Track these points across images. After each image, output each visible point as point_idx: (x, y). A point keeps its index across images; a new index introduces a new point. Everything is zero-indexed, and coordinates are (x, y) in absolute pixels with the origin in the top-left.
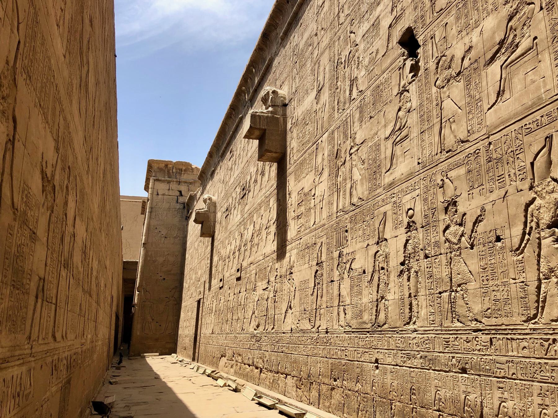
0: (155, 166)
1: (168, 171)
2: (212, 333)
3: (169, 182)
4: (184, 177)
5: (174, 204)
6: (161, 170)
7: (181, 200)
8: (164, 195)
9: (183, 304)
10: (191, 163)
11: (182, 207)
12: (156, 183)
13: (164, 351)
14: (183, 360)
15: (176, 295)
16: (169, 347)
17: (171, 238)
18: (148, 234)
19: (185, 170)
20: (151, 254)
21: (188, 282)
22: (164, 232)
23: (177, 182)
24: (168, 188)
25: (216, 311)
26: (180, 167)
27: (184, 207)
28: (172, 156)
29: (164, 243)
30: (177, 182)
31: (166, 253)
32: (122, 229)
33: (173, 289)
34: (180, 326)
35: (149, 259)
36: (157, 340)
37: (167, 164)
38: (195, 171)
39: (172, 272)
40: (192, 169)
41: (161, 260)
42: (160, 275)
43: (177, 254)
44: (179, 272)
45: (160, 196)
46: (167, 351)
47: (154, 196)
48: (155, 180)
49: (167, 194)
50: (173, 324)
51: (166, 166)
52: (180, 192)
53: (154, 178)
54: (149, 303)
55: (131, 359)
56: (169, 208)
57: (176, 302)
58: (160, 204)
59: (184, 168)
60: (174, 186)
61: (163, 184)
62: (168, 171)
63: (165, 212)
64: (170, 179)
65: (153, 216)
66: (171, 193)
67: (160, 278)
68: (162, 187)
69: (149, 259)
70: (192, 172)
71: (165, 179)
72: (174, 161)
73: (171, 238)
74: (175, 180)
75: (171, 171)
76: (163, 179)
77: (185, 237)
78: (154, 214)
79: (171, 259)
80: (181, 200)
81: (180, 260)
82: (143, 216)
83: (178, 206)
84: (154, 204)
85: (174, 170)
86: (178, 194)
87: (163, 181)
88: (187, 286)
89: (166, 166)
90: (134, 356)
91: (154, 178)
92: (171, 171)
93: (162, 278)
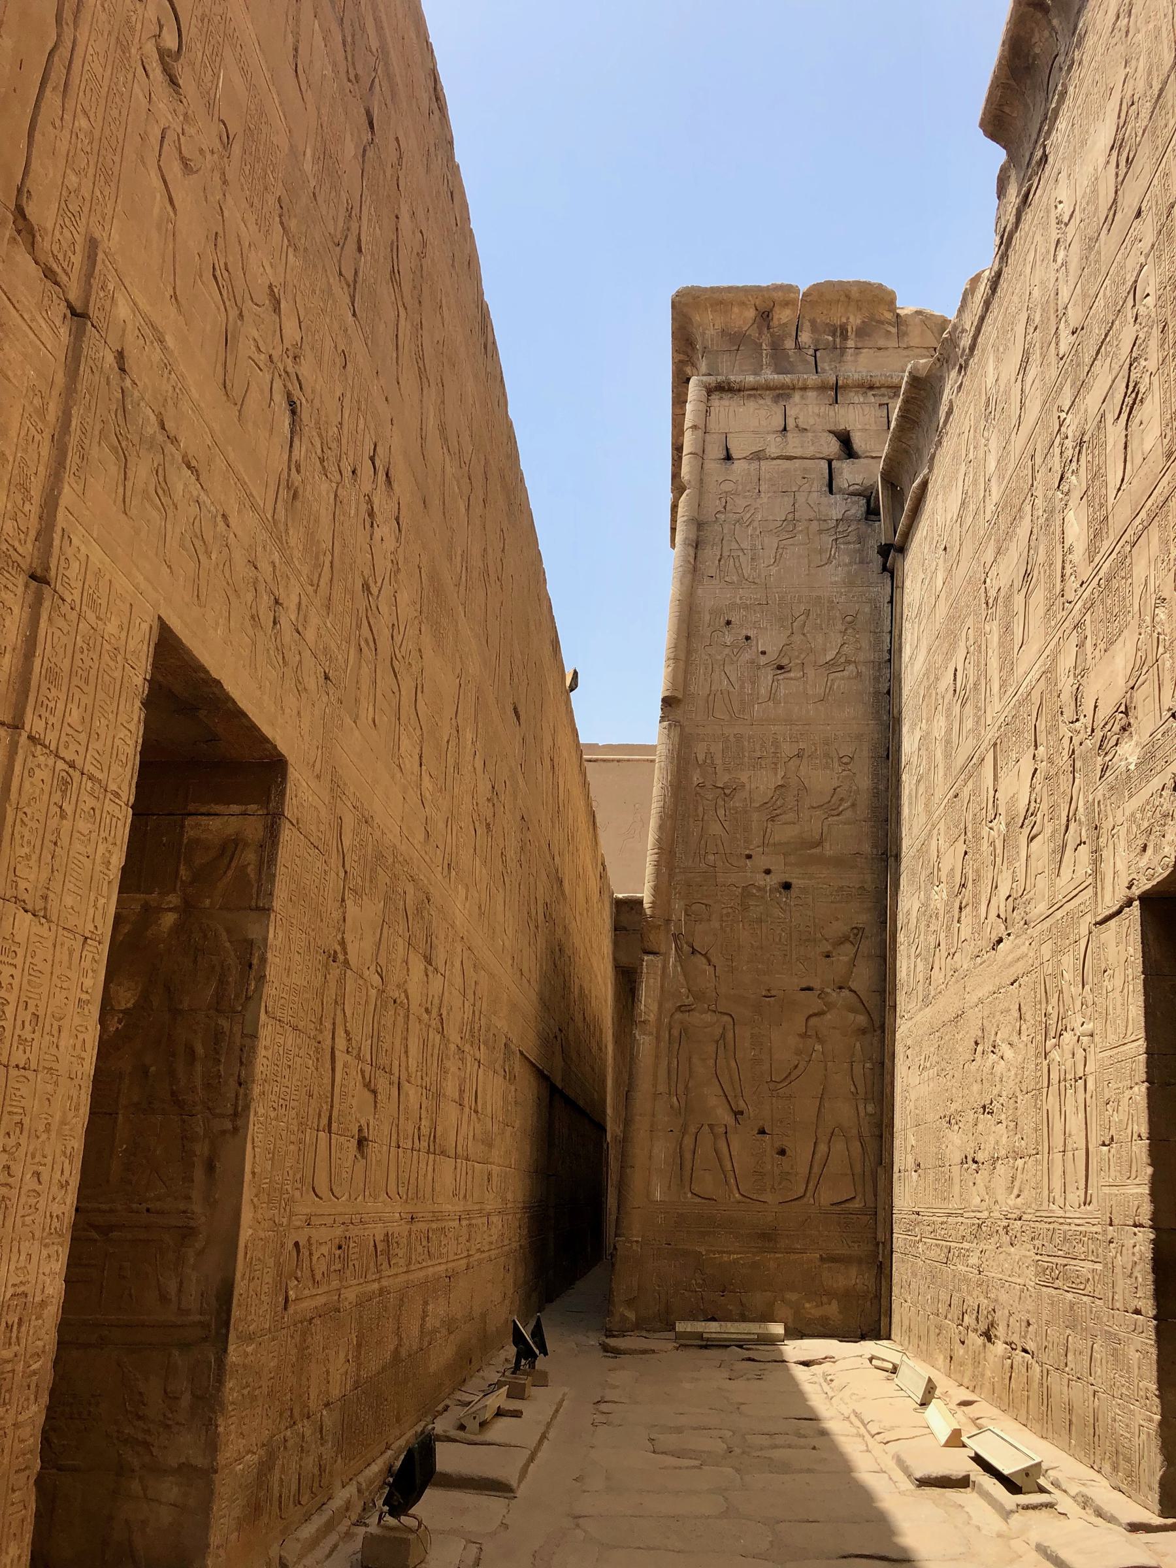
0: (708, 325)
1: (776, 347)
3: (781, 393)
4: (859, 365)
5: (813, 496)
6: (736, 340)
7: (850, 474)
8: (758, 456)
9: (911, 1024)
10: (889, 286)
11: (857, 508)
12: (715, 400)
13: (811, 1309)
14: (1033, 1472)
15: (862, 979)
16: (868, 1320)
17: (811, 672)
18: (689, 652)
19: (861, 333)
20: (708, 753)
21: (951, 860)
22: (770, 641)
23: (822, 388)
24: (778, 422)
26: (837, 316)
27: (872, 512)
28: (793, 260)
29: (772, 696)
30: (822, 388)
31: (788, 749)
32: (573, 686)
33: (844, 940)
34: (902, 1158)
35: (696, 778)
36: (767, 1237)
37: (766, 305)
38: (915, 337)
39: (829, 850)
40: (899, 320)
41: (762, 783)
42: (762, 862)
43: (847, 750)
44: (866, 848)
45: (739, 466)
46: (832, 1309)
47: (712, 466)
48: (710, 391)
49: (773, 451)
50: (856, 1146)
51: (765, 316)
52: (845, 440)
53: (705, 378)
54: (709, 1017)
55: (617, 1352)
56: (791, 522)
57: (862, 1020)
58: (741, 502)
59: (855, 321)
60: (809, 410)
61: (751, 405)
62: (776, 347)
63: (771, 542)
64: (787, 379)
65: (710, 563)
66: (794, 444)
67: (761, 880)
68: (747, 423)
69: (696, 778)
70: (900, 335)
71: (761, 379)
72: (803, 289)
73: (811, 672)
74: (812, 379)
75: (789, 344)
76: (751, 379)
77: (888, 662)
78: (710, 554)
79: (821, 780)
80: (850, 474)
81: (864, 782)
83: (836, 507)
84: (713, 505)
85: (805, 337)
86: (832, 447)
87: (755, 391)
88: (940, 896)
89: (765, 316)
90: (642, 1326)
91: (711, 380)
92: (789, 344)
93: (773, 881)
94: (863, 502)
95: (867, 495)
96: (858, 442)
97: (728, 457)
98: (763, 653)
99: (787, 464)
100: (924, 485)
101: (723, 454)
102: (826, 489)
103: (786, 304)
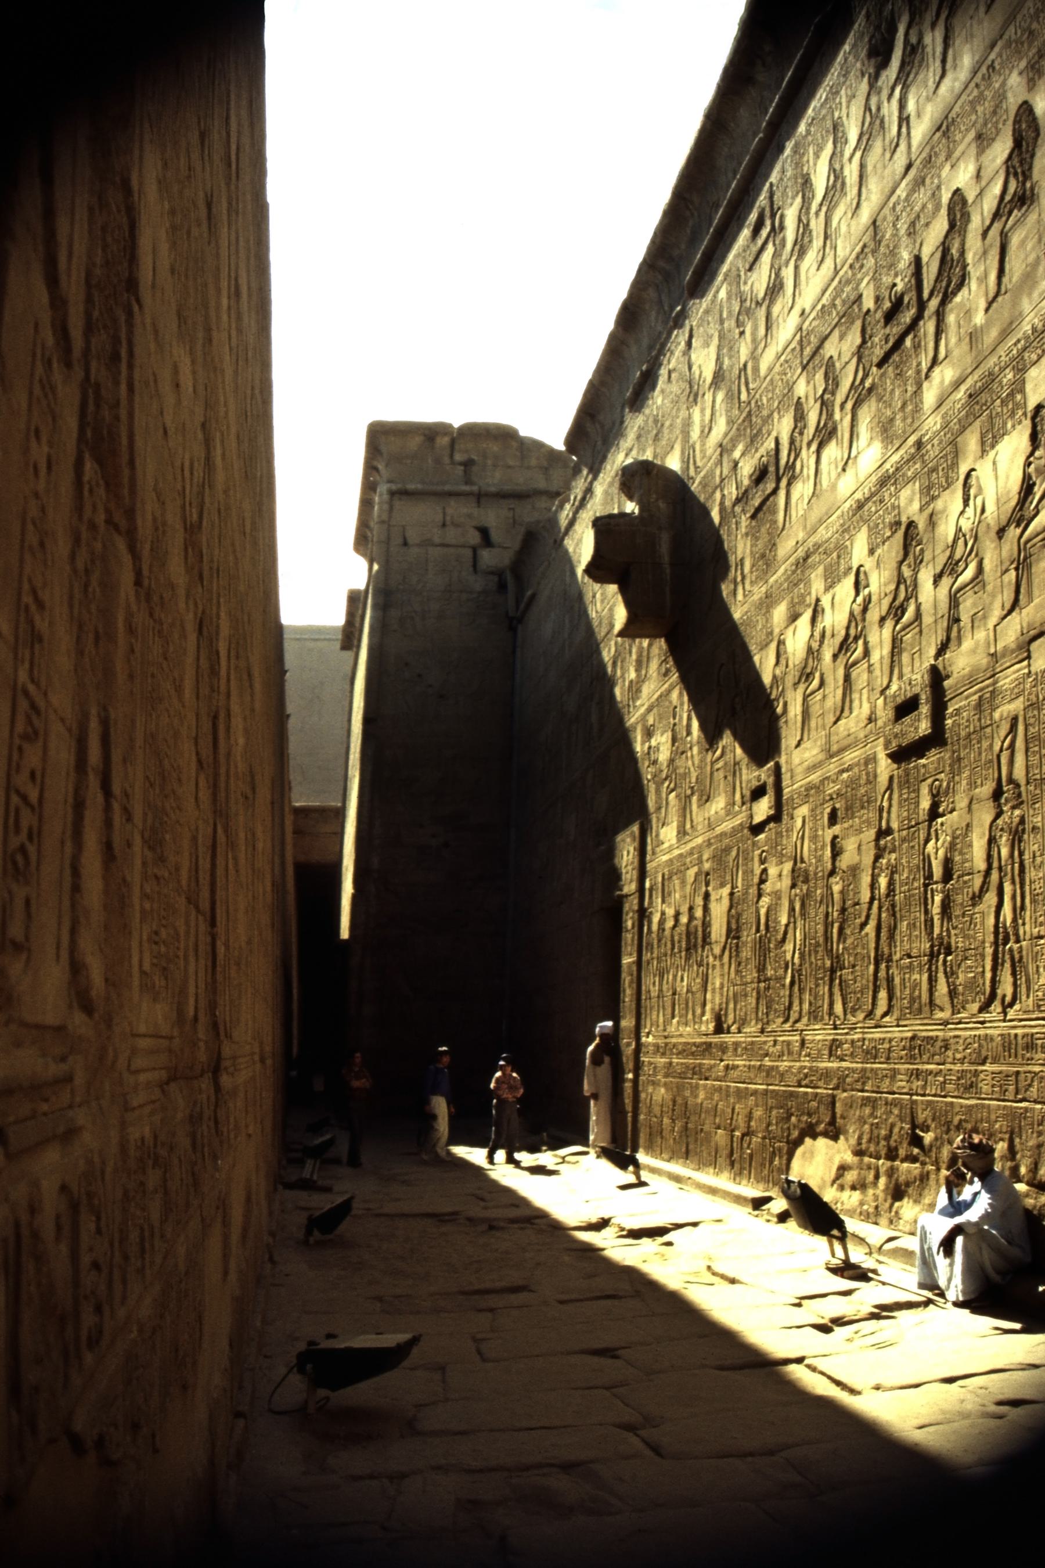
2: (719, 1029)
8: (426, 543)
12: (397, 504)
24: (439, 518)
25: (733, 932)
27: (502, 587)
45: (415, 551)
48: (392, 494)
52: (484, 532)
80: (488, 558)
82: (349, 655)
83: (478, 584)
86: (475, 538)
91: (394, 487)
92: (446, 460)
94: (496, 579)
95: (499, 574)
96: (495, 536)
97: (405, 544)
98: (430, 686)
99: (446, 550)
100: (533, 596)
101: (400, 541)
102: (471, 569)
103: (445, 434)
